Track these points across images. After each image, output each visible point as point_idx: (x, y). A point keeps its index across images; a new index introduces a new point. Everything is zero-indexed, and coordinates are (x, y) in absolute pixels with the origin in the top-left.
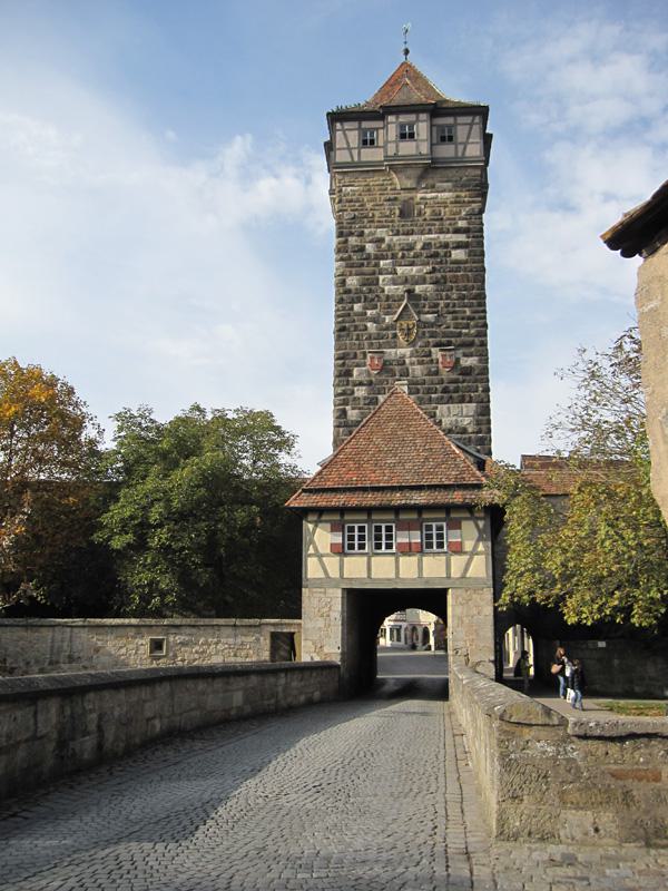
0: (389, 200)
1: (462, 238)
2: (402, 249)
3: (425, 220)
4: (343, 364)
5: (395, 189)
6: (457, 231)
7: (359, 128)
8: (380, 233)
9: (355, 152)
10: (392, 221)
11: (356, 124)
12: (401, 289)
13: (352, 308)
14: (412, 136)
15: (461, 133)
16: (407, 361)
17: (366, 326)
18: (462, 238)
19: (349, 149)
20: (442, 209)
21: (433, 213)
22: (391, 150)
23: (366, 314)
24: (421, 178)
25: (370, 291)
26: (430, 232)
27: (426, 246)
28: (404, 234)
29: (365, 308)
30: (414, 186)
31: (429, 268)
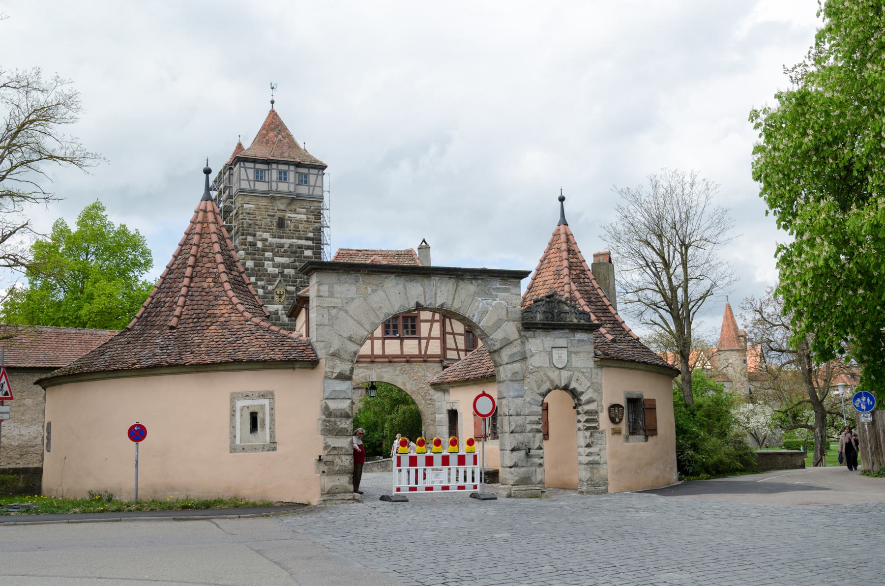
1: (310, 243)
6: (307, 239)
7: (254, 168)
8: (266, 235)
9: (252, 183)
11: (252, 165)
12: (277, 270)
14: (285, 179)
15: (312, 179)
16: (280, 312)
18: (310, 243)
19: (248, 180)
21: (296, 227)
22: (274, 188)
24: (290, 204)
26: (293, 238)
27: (291, 246)
29: (257, 280)
31: (292, 259)
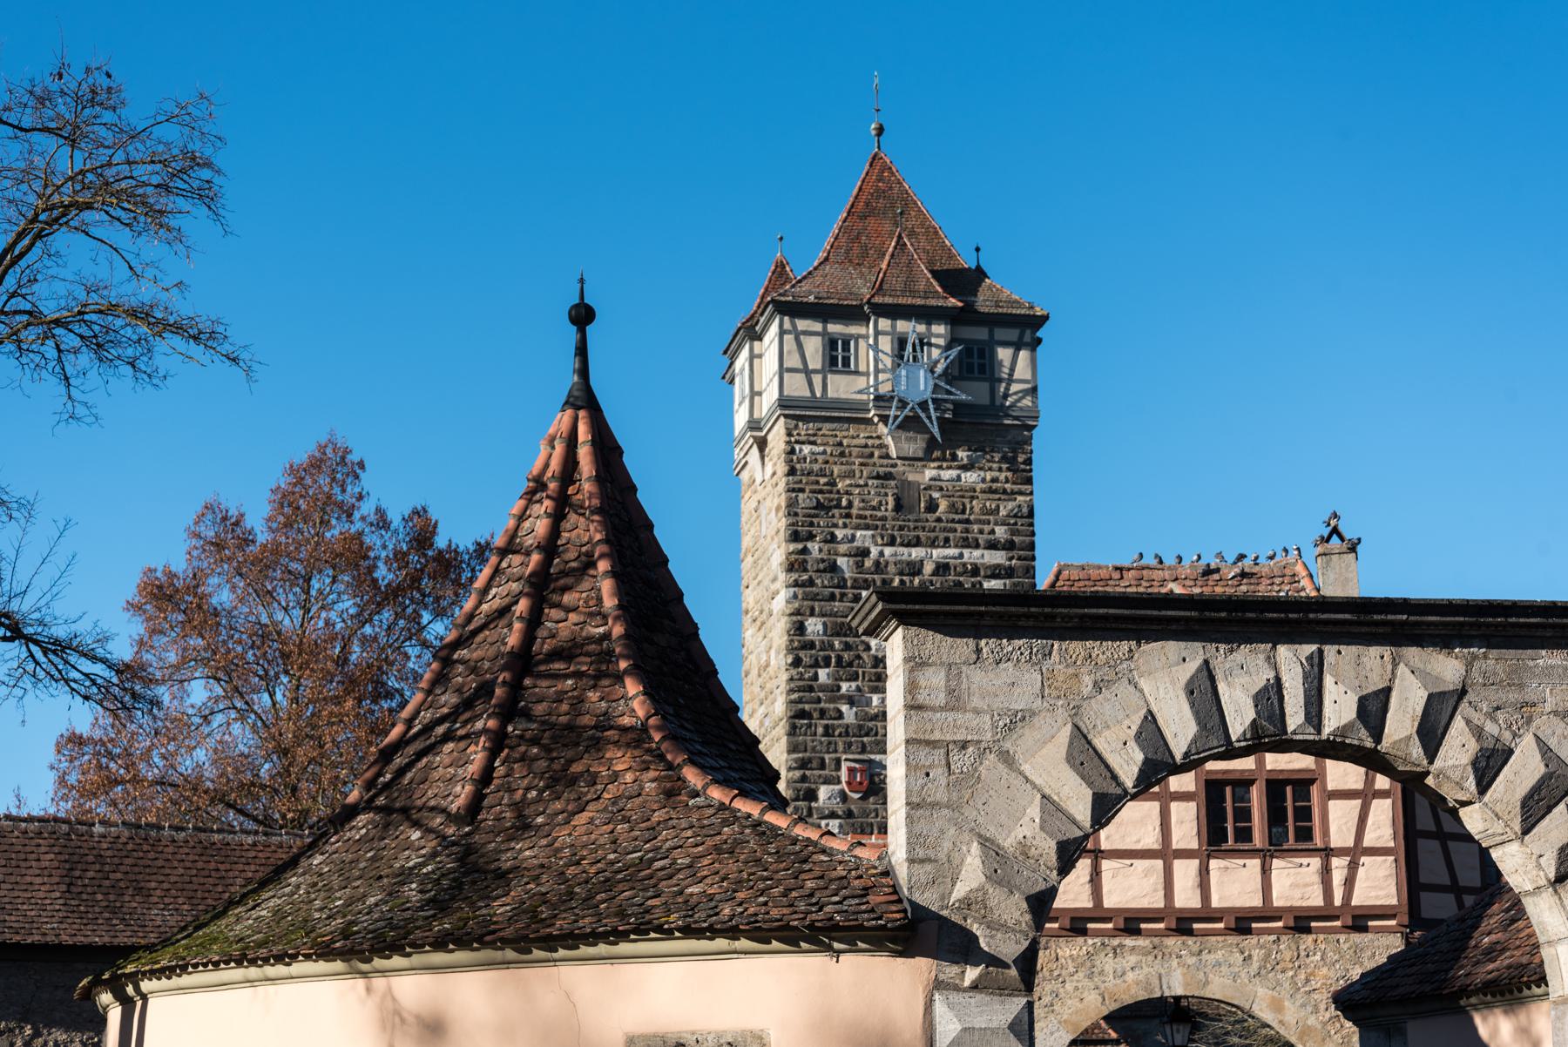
0: (878, 477)
1: (998, 558)
2: (901, 573)
3: (939, 520)
4: (804, 779)
5: (887, 456)
7: (824, 334)
9: (817, 380)
10: (884, 519)
11: (818, 327)
13: (816, 678)
17: (840, 711)
20: (967, 501)
21: (952, 508)
23: (839, 688)
25: (847, 647)
28: (902, 545)
30: (920, 454)
